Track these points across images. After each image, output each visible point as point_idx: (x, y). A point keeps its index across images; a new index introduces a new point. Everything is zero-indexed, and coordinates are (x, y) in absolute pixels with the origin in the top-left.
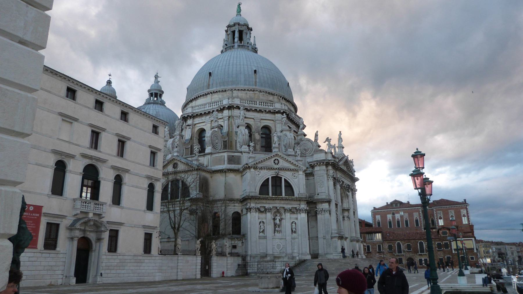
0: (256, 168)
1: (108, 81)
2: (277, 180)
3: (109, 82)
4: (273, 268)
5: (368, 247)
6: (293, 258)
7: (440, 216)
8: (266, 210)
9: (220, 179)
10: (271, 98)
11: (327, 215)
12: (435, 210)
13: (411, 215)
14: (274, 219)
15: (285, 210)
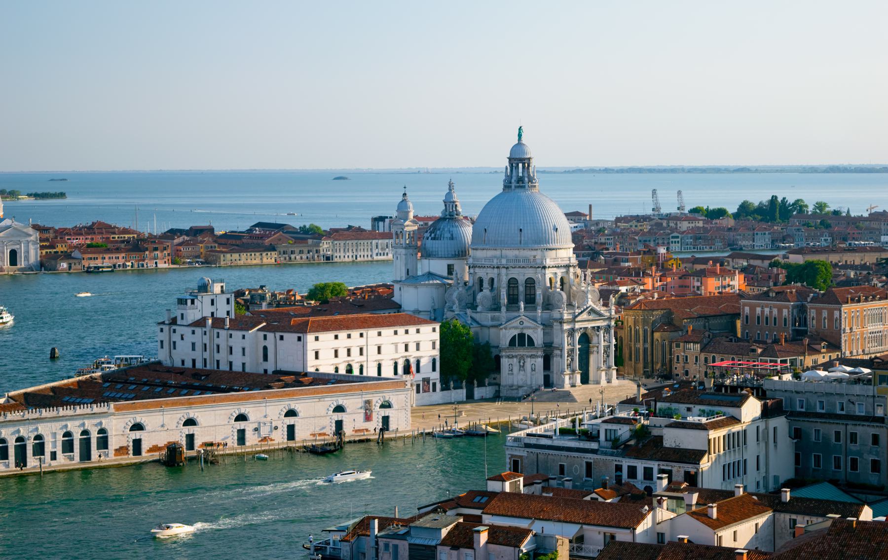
0: (506, 328)
1: (404, 194)
2: (522, 336)
3: (405, 195)
4: (517, 393)
5: (687, 357)
6: (532, 387)
7: (813, 317)
8: (513, 357)
9: (486, 330)
10: (534, 253)
11: (559, 358)
12: (809, 307)
13: (780, 311)
14: (520, 362)
15: (527, 357)
